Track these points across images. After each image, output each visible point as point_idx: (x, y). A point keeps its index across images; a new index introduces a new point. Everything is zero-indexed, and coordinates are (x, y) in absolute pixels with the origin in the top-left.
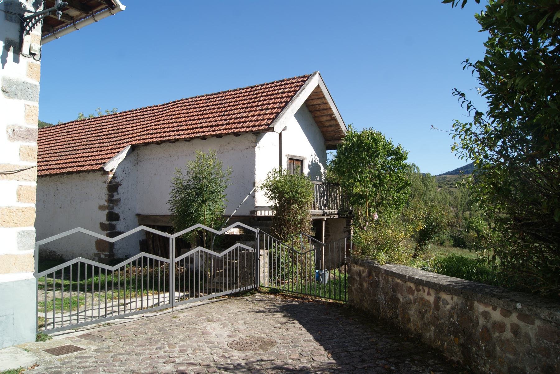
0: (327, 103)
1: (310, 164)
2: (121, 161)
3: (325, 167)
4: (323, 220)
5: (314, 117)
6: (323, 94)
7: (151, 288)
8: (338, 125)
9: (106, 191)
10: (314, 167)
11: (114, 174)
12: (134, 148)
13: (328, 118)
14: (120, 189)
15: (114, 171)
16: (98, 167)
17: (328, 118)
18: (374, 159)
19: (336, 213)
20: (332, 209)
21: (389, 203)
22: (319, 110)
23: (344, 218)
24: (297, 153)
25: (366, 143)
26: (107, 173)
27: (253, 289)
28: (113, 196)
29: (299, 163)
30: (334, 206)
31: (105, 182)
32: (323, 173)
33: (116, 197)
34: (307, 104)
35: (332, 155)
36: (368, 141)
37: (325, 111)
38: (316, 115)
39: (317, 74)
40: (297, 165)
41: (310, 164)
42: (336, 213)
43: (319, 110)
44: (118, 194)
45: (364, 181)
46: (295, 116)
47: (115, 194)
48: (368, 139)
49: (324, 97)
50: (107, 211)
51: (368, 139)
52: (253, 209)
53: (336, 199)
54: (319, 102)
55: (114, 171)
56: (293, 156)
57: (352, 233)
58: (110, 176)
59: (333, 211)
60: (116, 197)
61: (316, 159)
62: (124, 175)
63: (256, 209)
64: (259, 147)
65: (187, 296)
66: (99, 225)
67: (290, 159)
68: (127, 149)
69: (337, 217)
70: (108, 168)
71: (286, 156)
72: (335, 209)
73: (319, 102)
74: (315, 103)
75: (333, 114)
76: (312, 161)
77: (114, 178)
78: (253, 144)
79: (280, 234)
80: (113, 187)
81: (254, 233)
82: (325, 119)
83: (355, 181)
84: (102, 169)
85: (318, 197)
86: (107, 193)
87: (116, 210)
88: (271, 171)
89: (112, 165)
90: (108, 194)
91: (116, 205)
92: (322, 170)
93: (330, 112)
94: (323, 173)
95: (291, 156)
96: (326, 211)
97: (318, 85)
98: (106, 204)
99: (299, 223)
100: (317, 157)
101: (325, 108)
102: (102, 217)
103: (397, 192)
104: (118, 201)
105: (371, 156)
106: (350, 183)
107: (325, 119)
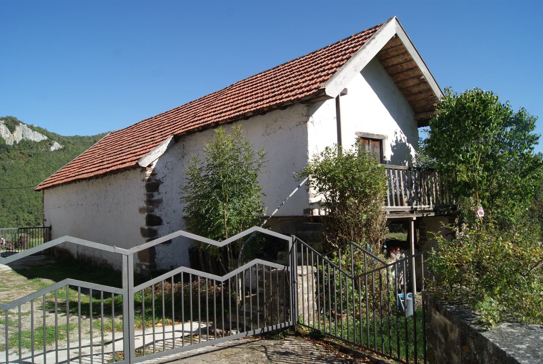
0: (411, 60)
1: (394, 144)
2: (160, 154)
3: (416, 148)
4: (411, 219)
5: (397, 83)
6: (404, 48)
8: (430, 90)
9: (144, 191)
10: (400, 150)
11: (153, 171)
12: (177, 139)
13: (416, 81)
14: (161, 188)
15: (153, 167)
16: (134, 163)
17: (416, 81)
18: (483, 129)
19: (431, 209)
20: (425, 205)
21: (510, 193)
22: (402, 72)
23: (445, 215)
24: (374, 130)
25: (469, 107)
26: (144, 169)
27: (286, 328)
28: (153, 196)
29: (377, 144)
30: (429, 200)
31: (143, 180)
32: (414, 156)
33: (156, 197)
35: (424, 133)
36: (472, 105)
37: (410, 72)
38: (399, 79)
39: (394, 20)
40: (374, 147)
41: (394, 144)
42: (431, 209)
43: (402, 72)
44: (159, 194)
45: (469, 163)
46: (362, 72)
47: (155, 193)
48: (472, 101)
49: (406, 52)
50: (146, 214)
51: (472, 101)
52: (307, 207)
55: (153, 167)
56: (368, 134)
58: (149, 172)
59: (427, 206)
60: (156, 197)
61: (403, 137)
62: (166, 171)
63: (311, 207)
65: (204, 331)
66: (139, 230)
68: (168, 141)
69: (433, 214)
70: (144, 163)
71: (356, 134)
72: (429, 204)
73: (400, 60)
76: (396, 141)
77: (153, 174)
78: (304, 119)
79: (334, 242)
80: (153, 185)
81: (287, 242)
82: (411, 83)
83: (456, 163)
84: (137, 166)
85: (402, 188)
86: (146, 192)
87: (157, 212)
88: (323, 149)
89: (151, 159)
90: (146, 194)
91: (157, 207)
92: (413, 153)
93: (417, 73)
94: (414, 156)
95: (364, 134)
96: (414, 207)
97: (396, 34)
98: (145, 205)
99: (365, 226)
100: (403, 135)
101: (410, 67)
102: (141, 221)
103: (522, 177)
104: (160, 201)
105: (478, 124)
106: (449, 166)
107: (411, 83)
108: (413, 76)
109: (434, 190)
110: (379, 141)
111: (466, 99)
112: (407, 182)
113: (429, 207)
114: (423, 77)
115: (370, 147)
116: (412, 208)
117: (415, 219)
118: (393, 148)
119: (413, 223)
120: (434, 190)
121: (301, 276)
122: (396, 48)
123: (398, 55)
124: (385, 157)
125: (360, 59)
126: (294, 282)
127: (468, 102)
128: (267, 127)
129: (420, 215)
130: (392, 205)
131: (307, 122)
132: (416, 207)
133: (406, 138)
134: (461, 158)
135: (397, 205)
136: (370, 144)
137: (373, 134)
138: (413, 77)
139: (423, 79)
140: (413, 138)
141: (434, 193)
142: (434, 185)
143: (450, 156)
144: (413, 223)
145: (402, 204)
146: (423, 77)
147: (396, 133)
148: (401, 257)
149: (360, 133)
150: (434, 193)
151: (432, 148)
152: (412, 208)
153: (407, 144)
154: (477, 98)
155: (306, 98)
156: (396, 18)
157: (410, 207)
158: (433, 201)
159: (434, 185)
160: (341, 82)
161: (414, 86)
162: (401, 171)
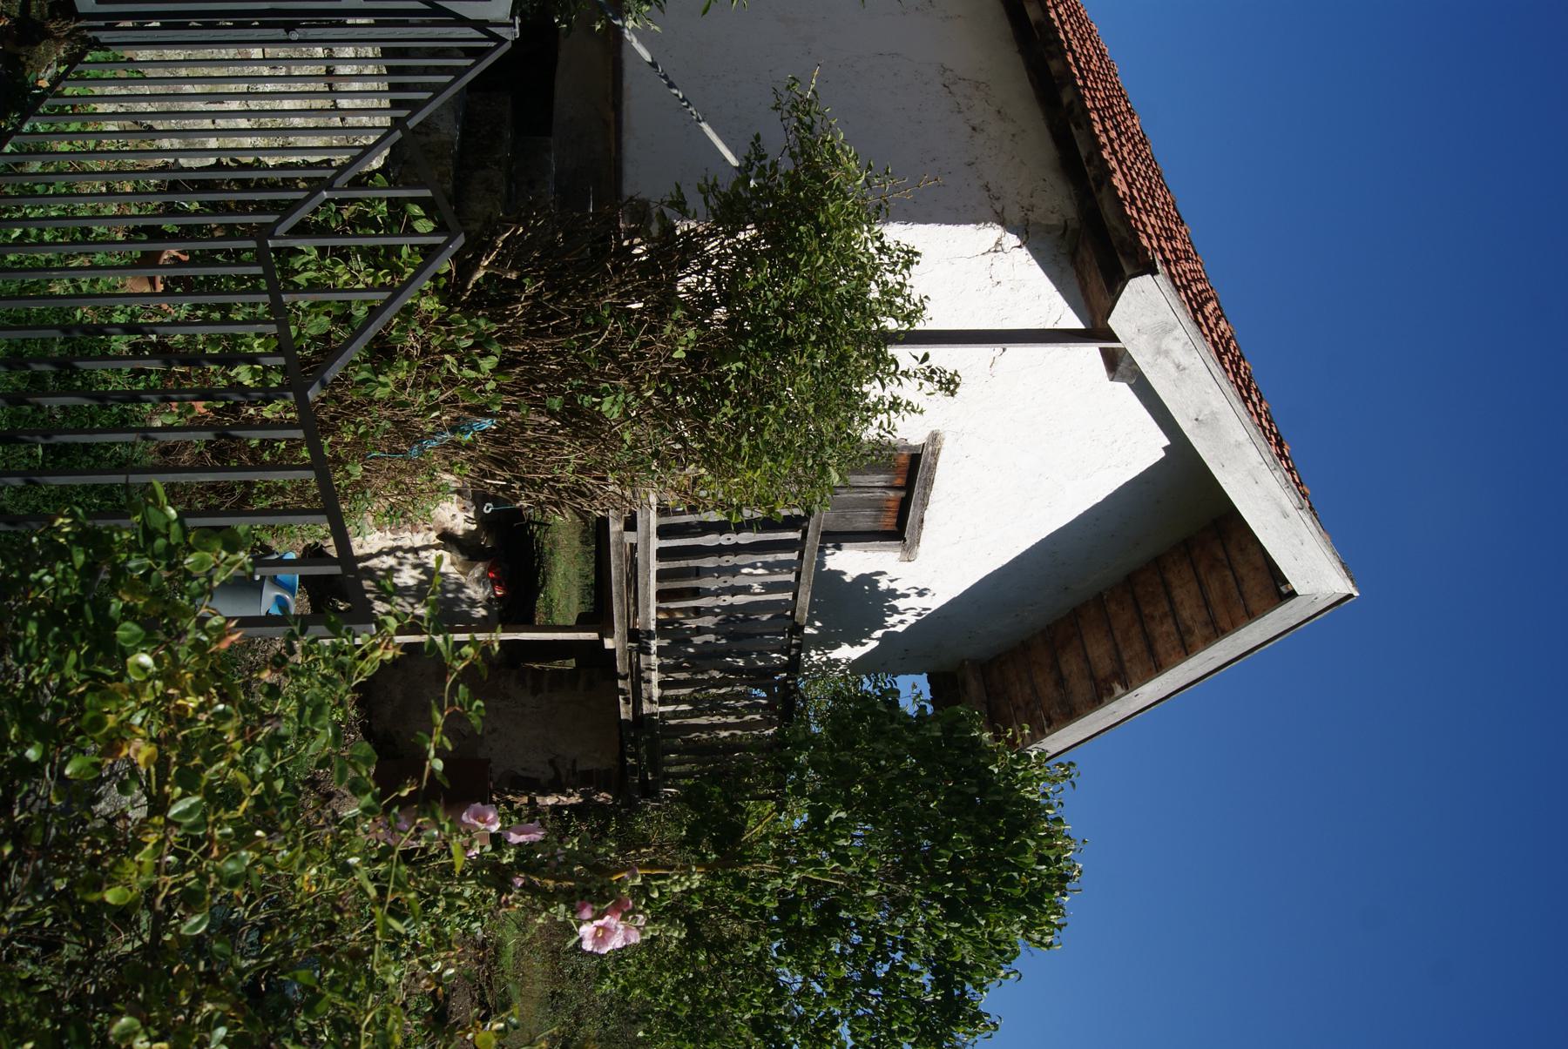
0: (1187, 651)
1: (883, 585)
3: (857, 666)
4: (607, 630)
5: (1099, 601)
6: (1235, 626)
8: (1071, 714)
10: (862, 604)
13: (1104, 666)
17: (1104, 666)
18: (937, 897)
19: (646, 708)
21: (700, 978)
25: (1023, 847)
29: (889, 522)
30: (677, 700)
34: (1225, 524)
36: (1029, 858)
37: (1138, 646)
38: (1113, 608)
40: (879, 507)
41: (883, 585)
42: (646, 708)
51: (1043, 860)
53: (715, 706)
54: (1189, 610)
56: (929, 483)
57: (550, 801)
59: (656, 693)
64: (998, 247)
69: (625, 712)
72: (663, 701)
73: (1189, 610)
74: (1179, 594)
75: (1128, 687)
76: (892, 593)
78: (1015, 214)
79: (499, 263)
83: (814, 797)
85: (728, 600)
92: (847, 653)
95: (932, 469)
96: (654, 644)
97: (1293, 594)
100: (911, 619)
101: (1160, 647)
103: (753, 1020)
105: (957, 880)
107: (1099, 651)
108: (1125, 658)
109: (716, 719)
110: (897, 528)
111: (1049, 836)
112: (746, 620)
113: (651, 701)
114: (1119, 690)
115: (878, 494)
116: (650, 635)
117: (609, 644)
118: (868, 580)
119: (594, 636)
120: (716, 719)
121: (330, 72)
122: (1235, 594)
123: (1207, 604)
124: (839, 548)
125: (1239, 445)
126: (289, 27)
127: (1039, 845)
128: (977, 85)
129: (621, 667)
130: (662, 554)
131: (1002, 223)
132: (654, 649)
133: (900, 628)
134: (833, 817)
135: (661, 576)
136: (891, 494)
137: (925, 505)
138: (1118, 653)
139: (1111, 692)
140: (900, 653)
141: (703, 721)
142: (732, 719)
143: (841, 775)
144: (594, 636)
145: (662, 595)
146: (1119, 690)
147: (921, 593)
148: (473, 603)
149: (935, 454)
150: (703, 721)
151: (863, 716)
152: (650, 635)
153: (878, 633)
154: (1049, 876)
155: (1107, 209)
156: (1351, 596)
157: (653, 627)
158: (675, 715)
159: (732, 719)
160: (1167, 353)
161: (1086, 659)
162: (789, 596)
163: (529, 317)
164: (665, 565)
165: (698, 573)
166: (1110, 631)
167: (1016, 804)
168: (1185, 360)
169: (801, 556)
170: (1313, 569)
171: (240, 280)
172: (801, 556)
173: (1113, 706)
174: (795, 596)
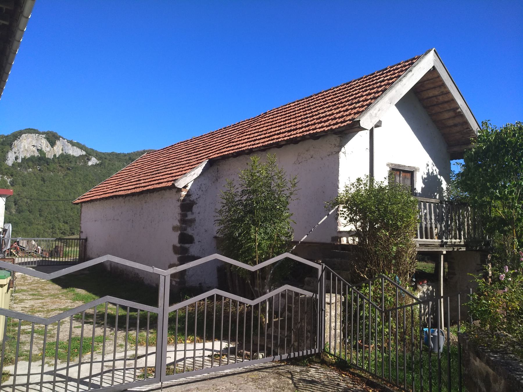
0: (448, 93)
1: (425, 176)
2: (195, 176)
3: (448, 181)
4: (441, 253)
5: (431, 115)
7: (191, 332)
8: (466, 123)
9: (178, 210)
10: (431, 182)
11: (188, 192)
12: (212, 163)
13: (451, 114)
14: (195, 209)
15: (188, 188)
16: (170, 184)
17: (451, 114)
19: (462, 243)
20: (456, 239)
22: (438, 104)
23: (476, 250)
24: (405, 161)
26: (179, 190)
27: (311, 355)
28: (186, 216)
29: (408, 175)
30: (460, 235)
31: (178, 200)
32: (445, 189)
33: (190, 217)
34: (417, 91)
35: (457, 166)
36: (513, 139)
37: (446, 105)
38: (433, 112)
39: (432, 52)
40: (404, 178)
41: (425, 176)
42: (462, 243)
43: (438, 104)
44: (193, 213)
45: (507, 199)
46: (396, 105)
47: (189, 213)
48: (514, 135)
49: (443, 85)
50: (179, 232)
51: (514, 135)
52: (335, 235)
53: (462, 224)
54: (436, 92)
55: (188, 188)
56: (399, 165)
57: (490, 273)
58: (184, 193)
59: (458, 240)
60: (190, 217)
62: (200, 193)
63: (339, 235)
64: (344, 153)
66: (171, 248)
67: (393, 169)
68: (204, 165)
69: (463, 249)
70: (180, 184)
71: (388, 165)
72: (460, 238)
73: (436, 92)
74: (431, 95)
75: (458, 107)
76: (428, 174)
77: (188, 195)
78: (336, 149)
79: (363, 273)
80: (187, 205)
81: (317, 270)
82: (446, 115)
83: (492, 199)
84: (173, 186)
85: (433, 221)
86: (180, 212)
87: (190, 231)
88: (354, 180)
89: (187, 181)
90: (180, 214)
91: (190, 226)
92: (444, 185)
93: (453, 106)
94: (445, 189)
95: (396, 165)
96: (445, 240)
97: (434, 67)
98: (179, 224)
99: (395, 258)
100: (435, 168)
102: (174, 238)
104: (193, 221)
106: (484, 201)
107: (446, 115)
108: (449, 108)
109: (466, 224)
110: (411, 173)
111: (506, 134)
112: (438, 216)
113: (461, 242)
114: (459, 110)
115: (401, 179)
116: (442, 241)
117: (445, 252)
118: (424, 180)
119: (442, 256)
120: (466, 224)
121: (328, 304)
122: (432, 81)
123: (435, 88)
124: (415, 189)
125: (396, 91)
126: (322, 310)
127: (509, 137)
128: (299, 155)
129: (451, 249)
130: (422, 238)
131: (339, 152)
132: (446, 240)
133: (438, 170)
134: (498, 194)
135: (427, 238)
136: (401, 175)
137: (405, 166)
138: (448, 110)
139: (460, 112)
140: (445, 171)
141: (466, 228)
142: (466, 220)
143: (484, 190)
144: (442, 256)
145: (432, 238)
146: (459, 110)
147: (428, 165)
148: (428, 290)
149: (392, 164)
150: (466, 228)
151: (465, 181)
152: (442, 241)
153: (439, 177)
154: (519, 133)
155: (340, 129)
156: (435, 50)
157: (440, 241)
158: (464, 236)
159: (466, 220)
160: (376, 114)
161: (449, 118)
162: (432, 204)
163: (375, 266)
164: (424, 237)
165: (426, 228)
166: (441, 113)
167: (496, 142)
168: (378, 109)
169: (422, 202)
170: (428, 62)
171: (366, 329)
172: (422, 202)
173: (464, 111)
174: (432, 203)
